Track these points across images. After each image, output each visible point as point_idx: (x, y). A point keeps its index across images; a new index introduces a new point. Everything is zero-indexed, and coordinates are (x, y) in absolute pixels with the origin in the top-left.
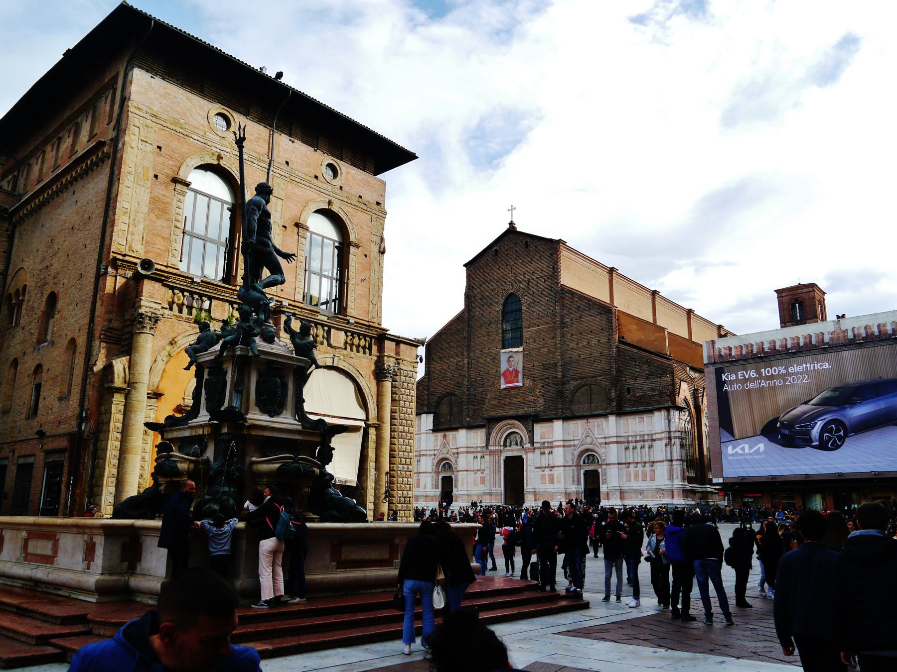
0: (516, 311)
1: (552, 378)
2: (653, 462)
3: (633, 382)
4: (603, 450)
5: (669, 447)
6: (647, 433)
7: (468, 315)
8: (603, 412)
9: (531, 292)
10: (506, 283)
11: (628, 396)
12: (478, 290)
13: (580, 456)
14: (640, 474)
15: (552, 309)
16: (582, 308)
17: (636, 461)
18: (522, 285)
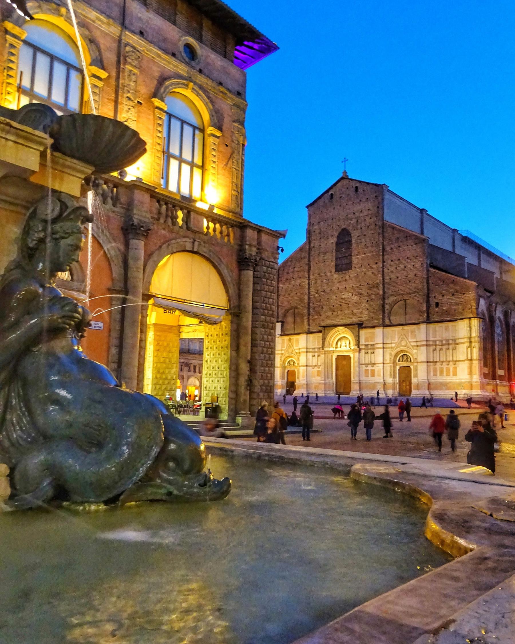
0: (347, 242)
1: (375, 295)
2: (456, 361)
3: (441, 298)
4: (415, 351)
5: (469, 349)
6: (451, 338)
7: (309, 246)
8: (416, 321)
9: (359, 226)
10: (339, 220)
11: (437, 309)
12: (316, 227)
13: (396, 356)
14: (445, 370)
15: (376, 240)
16: (401, 239)
17: (442, 360)
18: (352, 222)
